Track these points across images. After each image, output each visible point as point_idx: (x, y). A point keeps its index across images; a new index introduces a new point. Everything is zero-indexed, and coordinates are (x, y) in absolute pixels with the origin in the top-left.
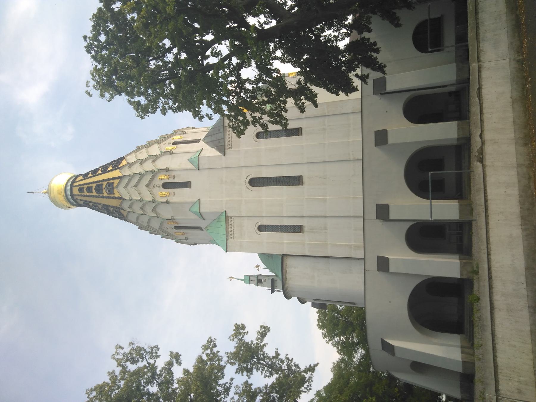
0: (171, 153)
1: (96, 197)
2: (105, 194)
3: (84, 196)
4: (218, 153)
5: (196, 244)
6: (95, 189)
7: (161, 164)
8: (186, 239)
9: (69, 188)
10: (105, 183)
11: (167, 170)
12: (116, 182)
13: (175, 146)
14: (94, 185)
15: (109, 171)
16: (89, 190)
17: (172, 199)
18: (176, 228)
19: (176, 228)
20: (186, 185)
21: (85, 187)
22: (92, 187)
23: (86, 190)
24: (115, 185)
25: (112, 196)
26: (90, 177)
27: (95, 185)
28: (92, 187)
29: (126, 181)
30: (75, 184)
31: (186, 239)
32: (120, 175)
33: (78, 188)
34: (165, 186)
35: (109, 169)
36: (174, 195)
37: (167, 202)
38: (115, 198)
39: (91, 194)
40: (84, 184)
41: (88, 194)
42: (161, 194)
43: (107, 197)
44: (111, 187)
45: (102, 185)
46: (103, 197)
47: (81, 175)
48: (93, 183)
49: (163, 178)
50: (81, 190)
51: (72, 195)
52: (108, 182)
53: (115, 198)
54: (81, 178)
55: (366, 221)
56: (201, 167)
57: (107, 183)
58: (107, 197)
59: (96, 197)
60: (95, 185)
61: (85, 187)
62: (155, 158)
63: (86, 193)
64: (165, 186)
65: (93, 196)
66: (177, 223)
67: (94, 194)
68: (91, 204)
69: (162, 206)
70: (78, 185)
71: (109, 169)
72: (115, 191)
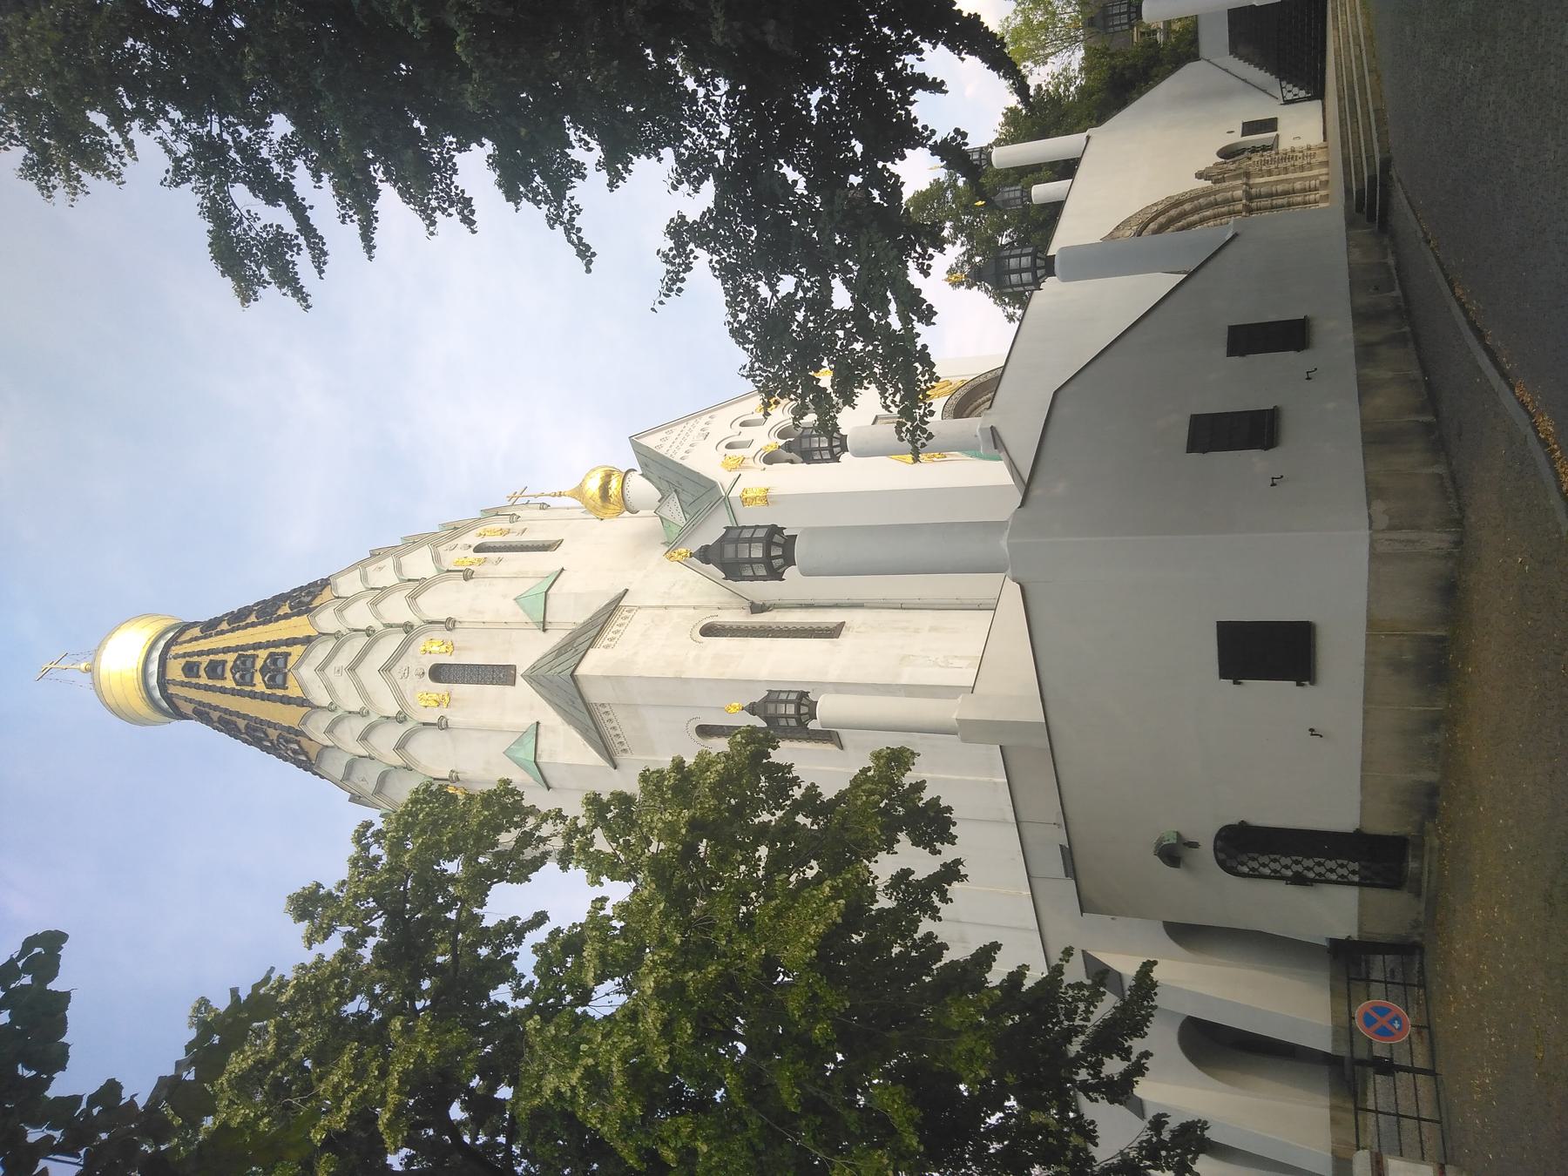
1: (233, 692)
2: (260, 687)
3: (198, 687)
7: (434, 605)
10: (263, 654)
11: (450, 624)
12: (297, 651)
13: (482, 555)
14: (231, 658)
15: (279, 618)
16: (215, 670)
20: (502, 675)
21: (205, 660)
22: (224, 662)
24: (292, 661)
25: (280, 692)
26: (222, 632)
28: (224, 662)
29: (321, 651)
30: (175, 650)
33: (183, 661)
34: (439, 673)
35: (280, 612)
37: (442, 725)
38: (287, 701)
39: (219, 684)
40: (201, 653)
41: (210, 683)
42: (425, 697)
43: (263, 697)
44: (276, 671)
45: (255, 657)
46: (253, 695)
47: (195, 624)
48: (227, 650)
49: (432, 650)
50: (190, 669)
53: (287, 701)
55: (1023, 826)
57: (271, 655)
58: (263, 697)
59: (233, 692)
61: (205, 660)
63: (204, 680)
64: (439, 673)
65: (223, 690)
67: (229, 683)
68: (215, 715)
69: (429, 736)
70: (185, 655)
71: (280, 612)
72: (291, 682)
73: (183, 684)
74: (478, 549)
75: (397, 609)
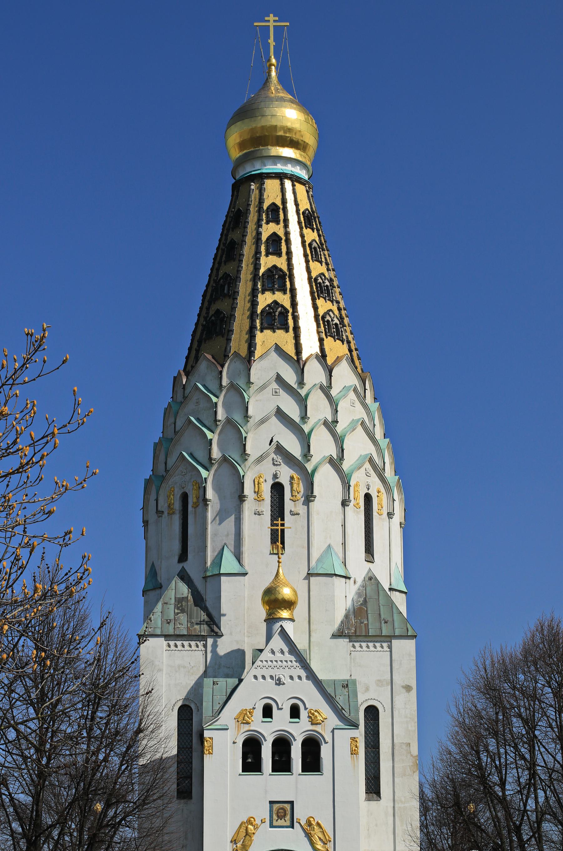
0: (345, 503)
4: (339, 616)
5: (146, 523)
6: (275, 267)
7: (326, 482)
8: (159, 513)
9: (279, 168)
10: (284, 300)
11: (309, 498)
15: (315, 307)
17: (248, 507)
18: (185, 497)
19: (185, 497)
23: (274, 234)
27: (285, 268)
28: (279, 255)
30: (288, 184)
31: (159, 513)
32: (304, 356)
33: (279, 203)
34: (277, 489)
35: (320, 302)
36: (258, 513)
41: (264, 237)
43: (254, 303)
46: (254, 294)
51: (261, 178)
52: (291, 311)
54: (305, 205)
56: (312, 579)
59: (257, 267)
60: (285, 268)
62: (336, 463)
66: (196, 506)
70: (284, 201)
73: (261, 201)
74: (368, 498)
75: (322, 445)
